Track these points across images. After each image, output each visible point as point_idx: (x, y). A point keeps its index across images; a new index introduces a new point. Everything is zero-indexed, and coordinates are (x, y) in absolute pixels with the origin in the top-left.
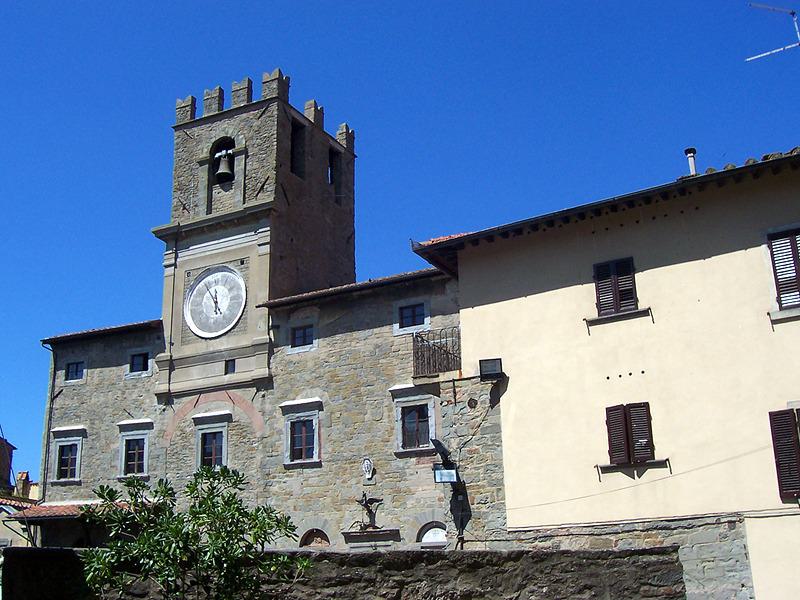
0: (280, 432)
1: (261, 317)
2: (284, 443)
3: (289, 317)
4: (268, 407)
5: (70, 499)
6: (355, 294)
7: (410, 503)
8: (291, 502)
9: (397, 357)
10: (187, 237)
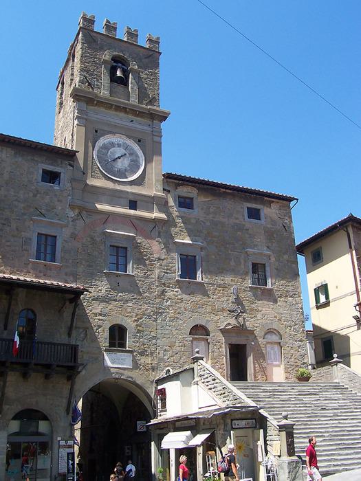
6: (222, 190)
7: (259, 316)
9: (247, 233)
10: (96, 104)
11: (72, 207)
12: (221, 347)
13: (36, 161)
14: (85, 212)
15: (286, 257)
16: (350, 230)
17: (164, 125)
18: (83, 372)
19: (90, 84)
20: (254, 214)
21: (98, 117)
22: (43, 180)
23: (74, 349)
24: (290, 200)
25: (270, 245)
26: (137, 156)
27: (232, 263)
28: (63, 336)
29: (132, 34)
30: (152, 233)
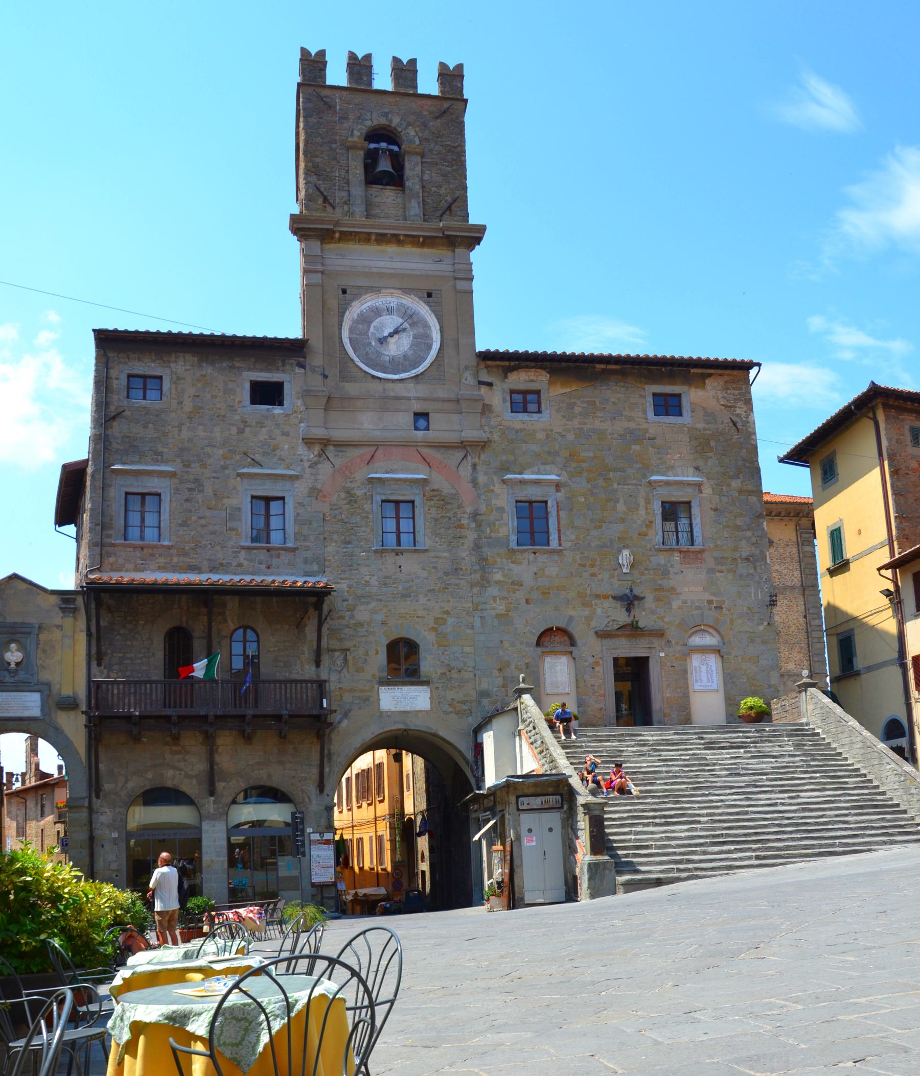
0: (501, 510)
1: (466, 368)
2: (508, 527)
3: (506, 377)
4: (482, 479)
5: (153, 571)
7: (676, 604)
8: (521, 595)
10: (340, 240)
11: (309, 442)
12: (597, 663)
13: (239, 368)
14: (331, 448)
15: (736, 484)
16: (881, 416)
17: (477, 256)
18: (345, 723)
19: (325, 199)
20: (668, 405)
21: (346, 262)
22: (254, 401)
23: (321, 685)
24: (746, 366)
25: (701, 463)
26: (426, 326)
27: (621, 507)
28: (307, 667)
29: (405, 71)
30: (461, 468)
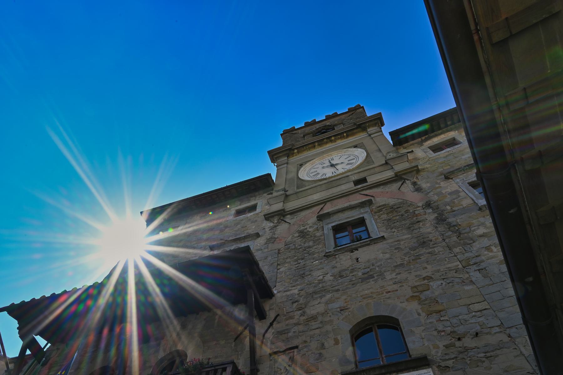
10: (298, 152)
